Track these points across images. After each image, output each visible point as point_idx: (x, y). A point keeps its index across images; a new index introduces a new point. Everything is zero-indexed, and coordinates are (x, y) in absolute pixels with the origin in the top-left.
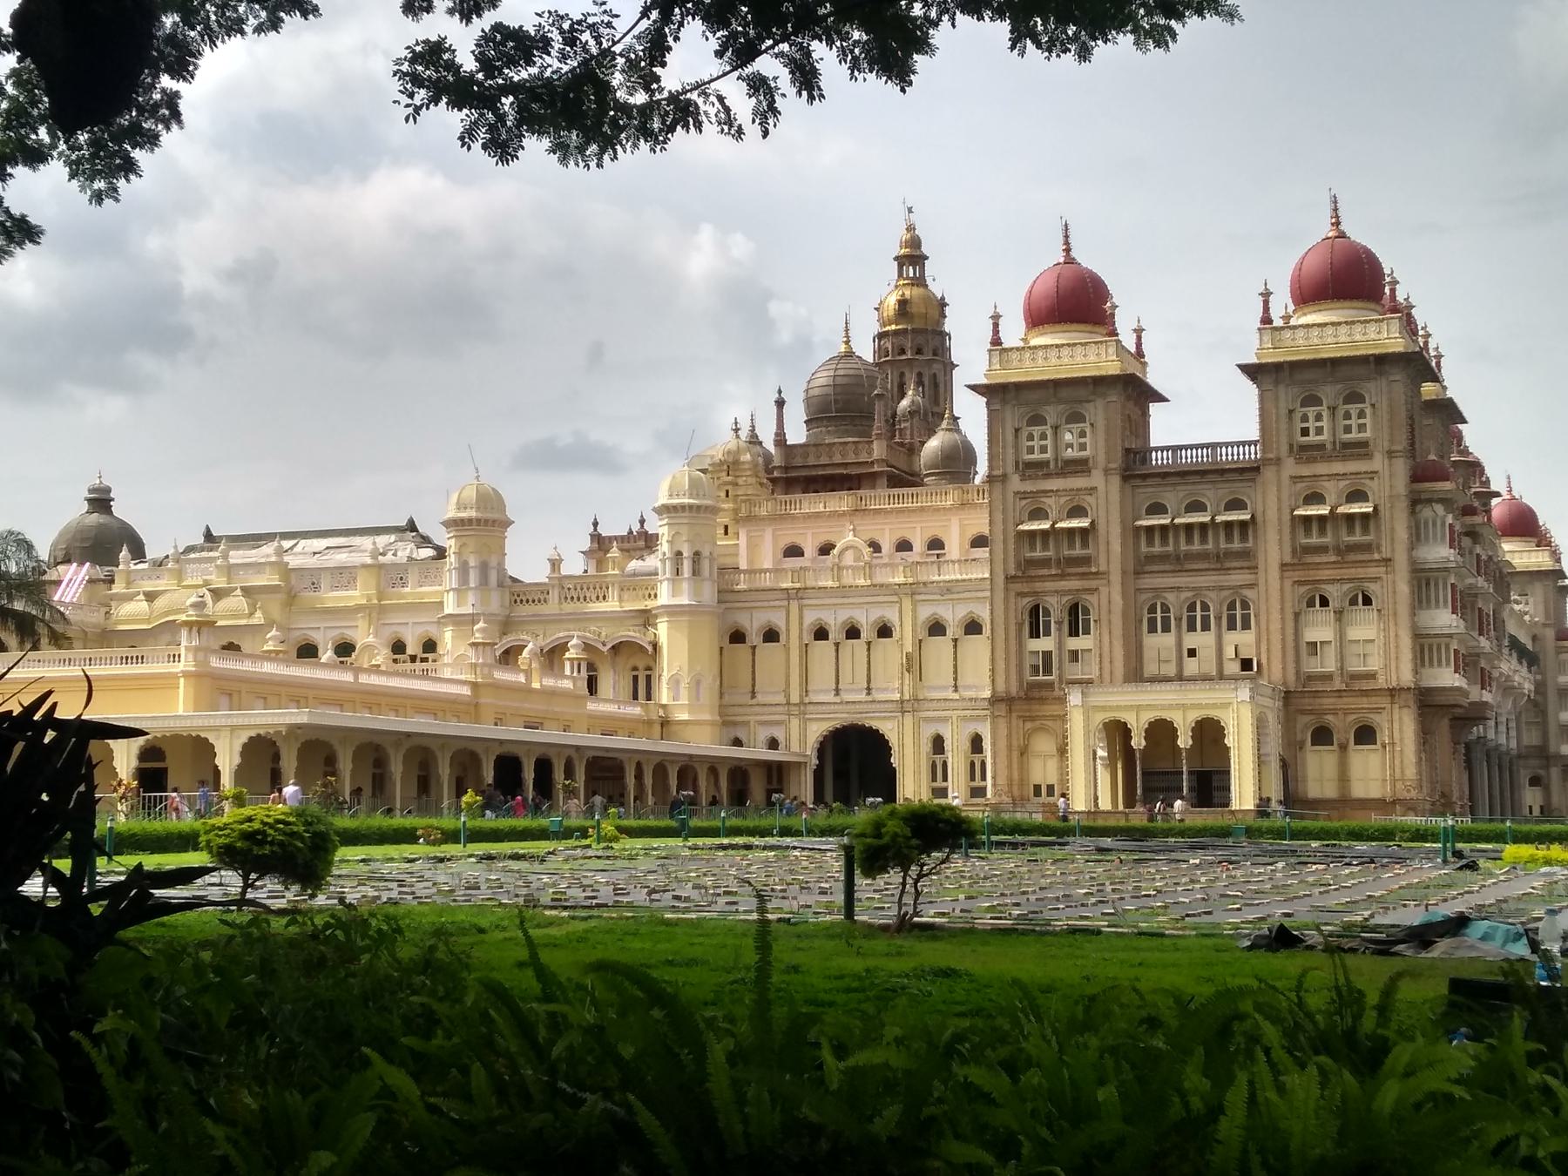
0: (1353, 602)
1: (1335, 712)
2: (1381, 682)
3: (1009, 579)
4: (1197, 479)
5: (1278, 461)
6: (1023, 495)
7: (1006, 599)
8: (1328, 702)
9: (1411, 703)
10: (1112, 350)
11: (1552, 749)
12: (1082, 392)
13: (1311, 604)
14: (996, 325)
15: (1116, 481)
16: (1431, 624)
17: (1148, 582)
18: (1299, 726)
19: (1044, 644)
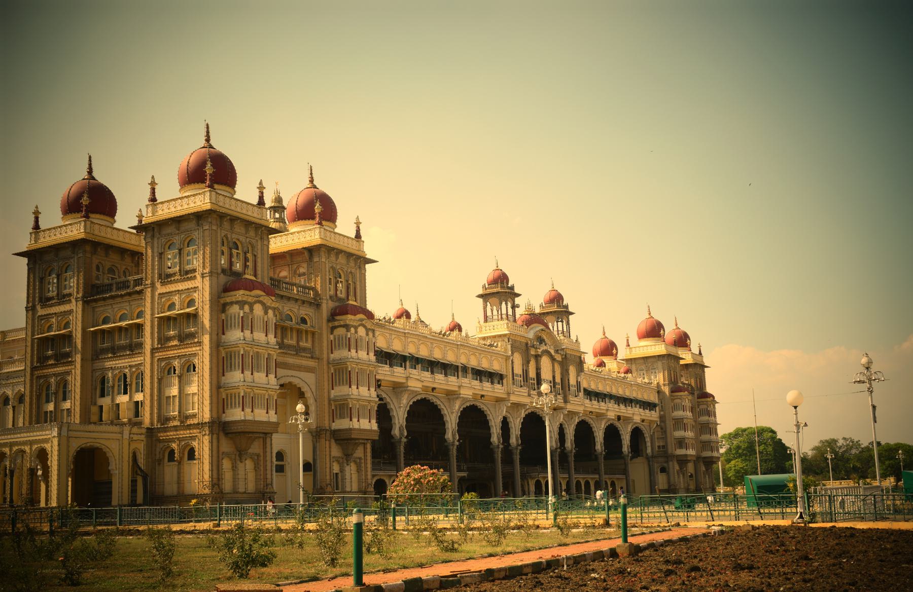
0: (188, 370)
1: (173, 440)
2: (195, 421)
3: (33, 369)
4: (119, 300)
5: (153, 285)
6: (41, 318)
7: (32, 380)
8: (171, 434)
9: (207, 432)
10: (82, 227)
11: (670, 451)
12: (68, 253)
13: (169, 373)
14: (37, 219)
15: (80, 304)
16: (231, 381)
17: (98, 365)
18: (158, 450)
19: (51, 407)
